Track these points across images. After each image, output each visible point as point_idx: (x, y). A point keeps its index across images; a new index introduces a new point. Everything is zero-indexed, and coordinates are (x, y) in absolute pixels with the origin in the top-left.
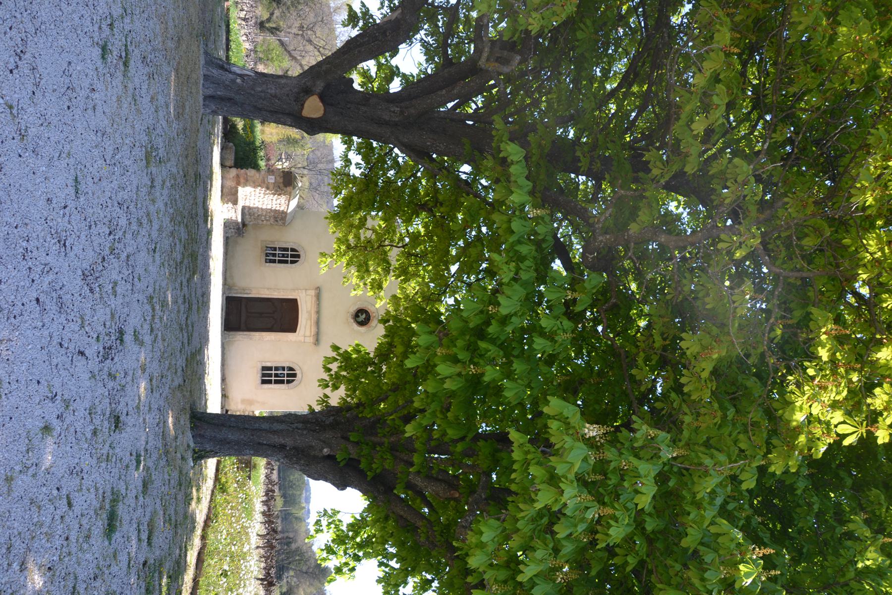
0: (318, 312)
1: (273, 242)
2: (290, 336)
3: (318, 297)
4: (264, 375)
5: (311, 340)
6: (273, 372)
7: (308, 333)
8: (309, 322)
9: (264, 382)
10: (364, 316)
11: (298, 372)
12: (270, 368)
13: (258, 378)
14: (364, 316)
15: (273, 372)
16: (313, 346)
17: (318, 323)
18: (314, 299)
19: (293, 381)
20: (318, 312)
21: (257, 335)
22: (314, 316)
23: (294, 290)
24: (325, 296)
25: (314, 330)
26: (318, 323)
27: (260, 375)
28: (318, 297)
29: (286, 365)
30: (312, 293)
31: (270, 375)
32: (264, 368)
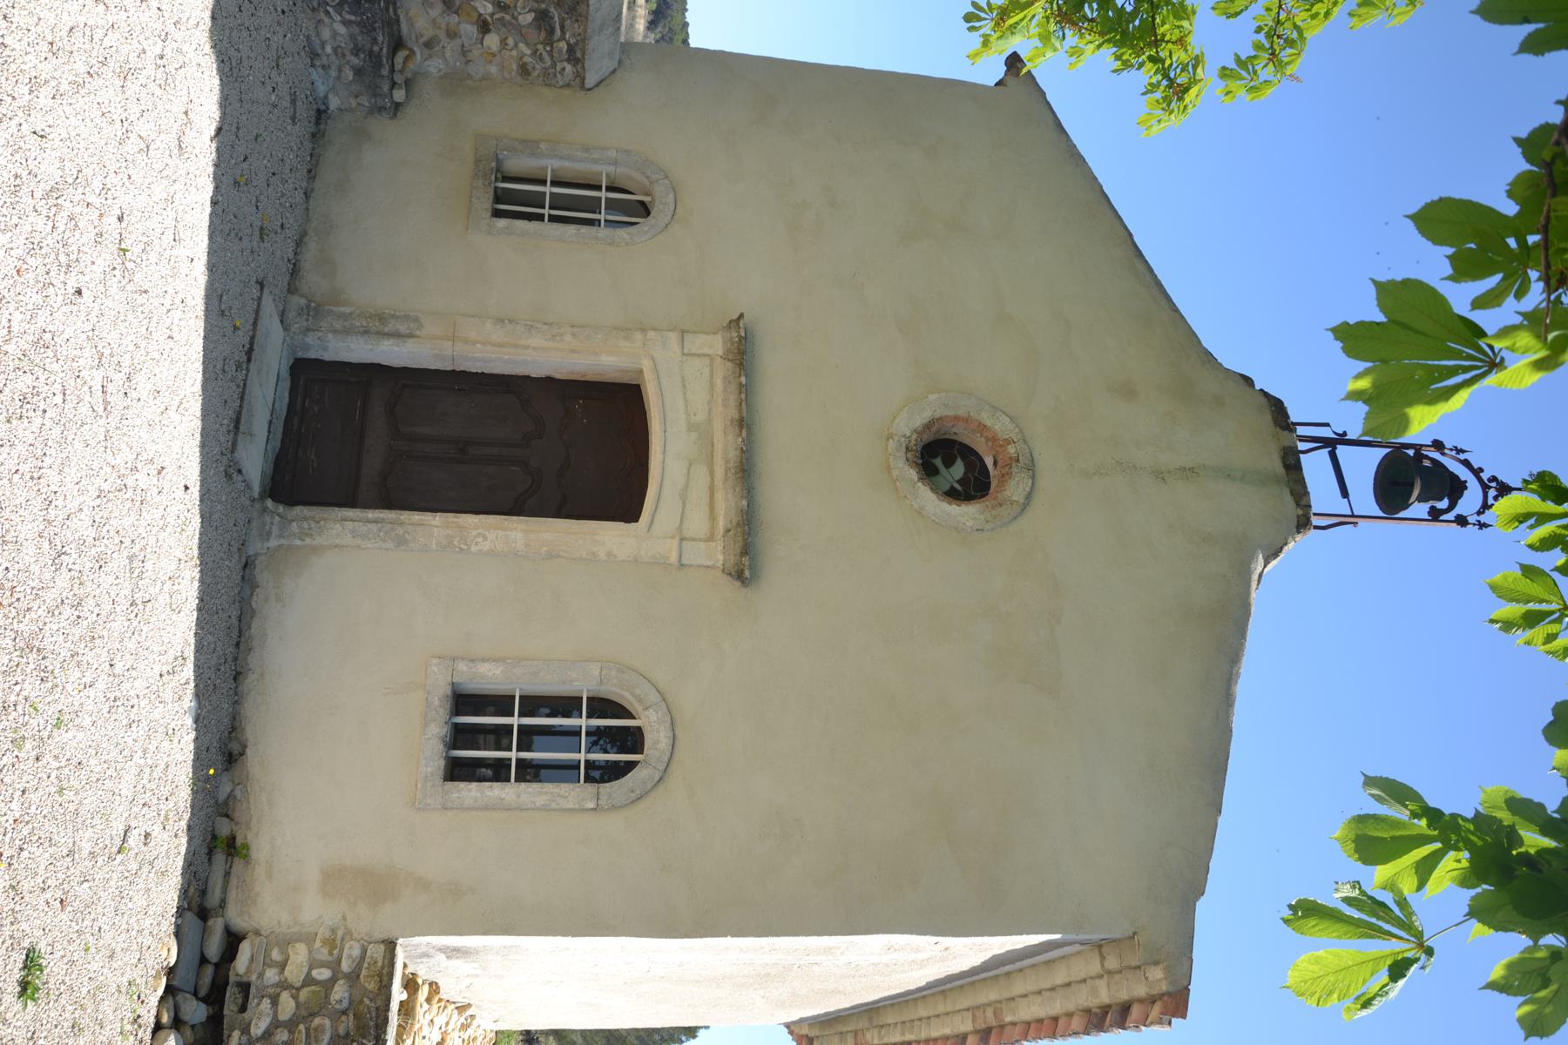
0: (745, 423)
1: (531, 146)
2: (608, 536)
3: (743, 353)
4: (461, 736)
5: (717, 554)
6: (515, 721)
7: (697, 523)
8: (701, 473)
9: (458, 771)
10: (958, 470)
11: (649, 721)
12: (501, 704)
13: (427, 743)
14: (958, 470)
15: (515, 721)
16: (730, 588)
17: (746, 471)
18: (723, 369)
19: (631, 766)
20: (745, 423)
21: (434, 528)
22: (725, 445)
23: (624, 330)
24: (773, 362)
25: (727, 505)
26: (746, 471)
27: (438, 729)
28: (743, 353)
29: (582, 684)
30: (715, 345)
31: (500, 736)
32: (464, 701)
